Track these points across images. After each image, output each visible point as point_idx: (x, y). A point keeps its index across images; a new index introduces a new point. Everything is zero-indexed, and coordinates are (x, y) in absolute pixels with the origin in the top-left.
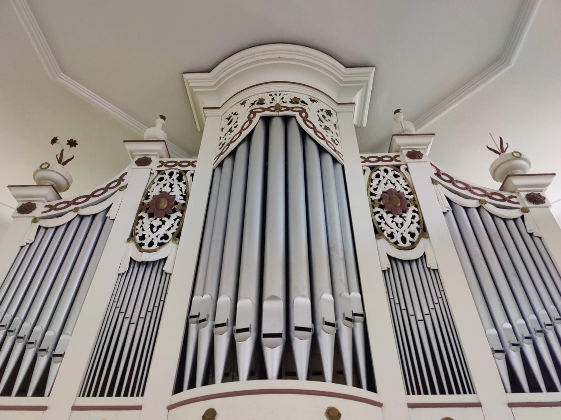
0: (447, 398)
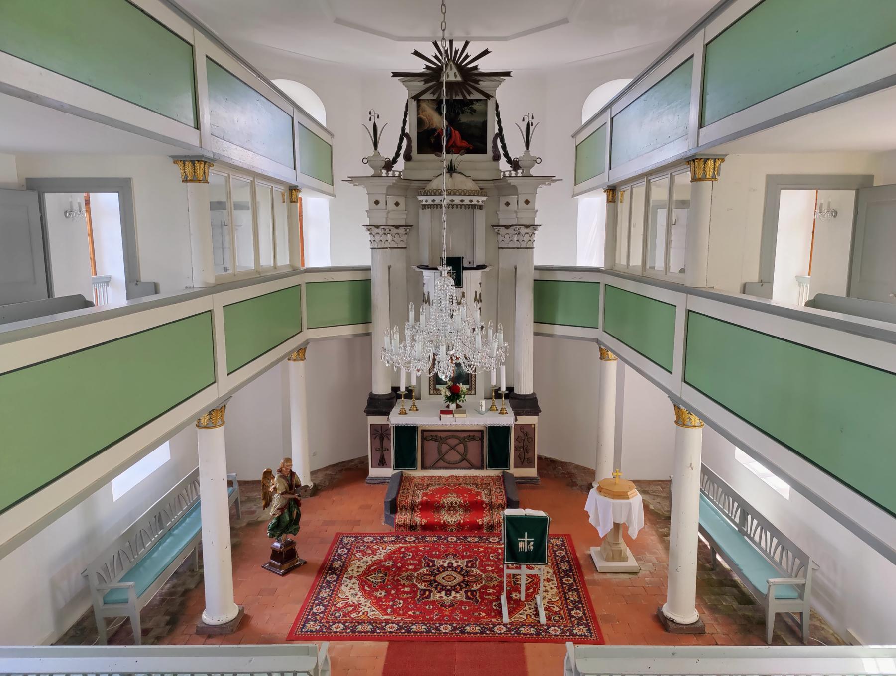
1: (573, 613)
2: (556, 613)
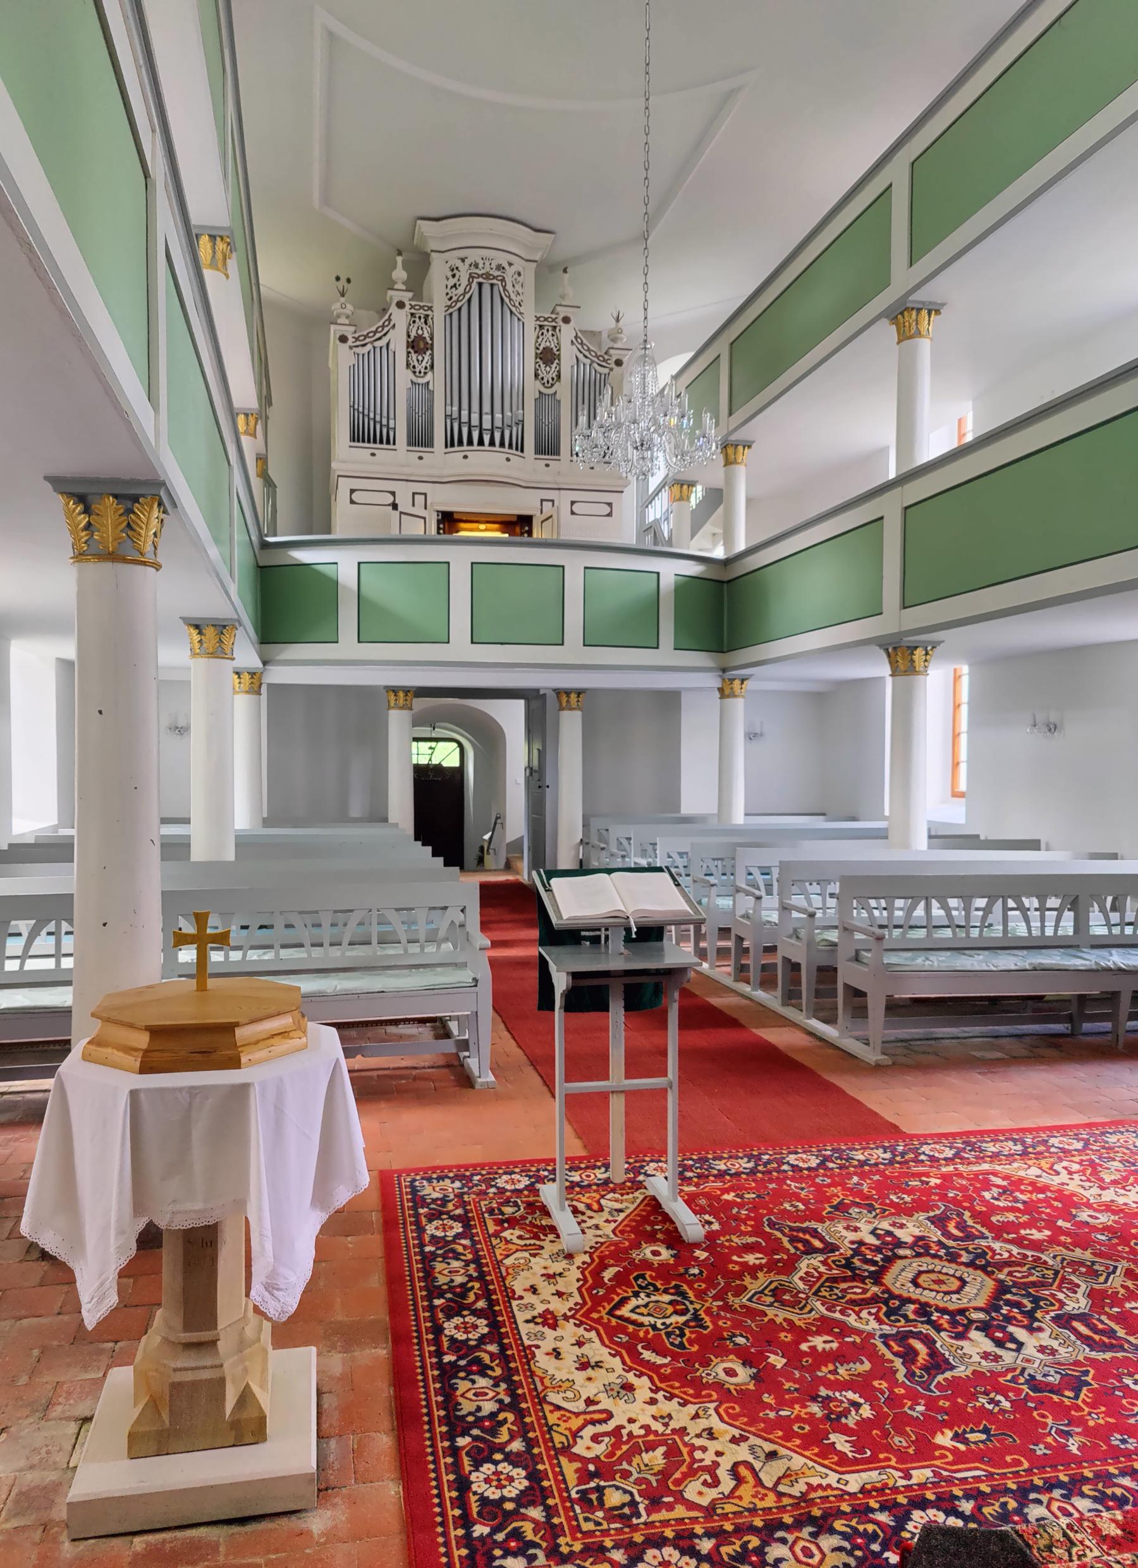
0: (549, 457)
1: (458, 1228)
2: (513, 1222)
